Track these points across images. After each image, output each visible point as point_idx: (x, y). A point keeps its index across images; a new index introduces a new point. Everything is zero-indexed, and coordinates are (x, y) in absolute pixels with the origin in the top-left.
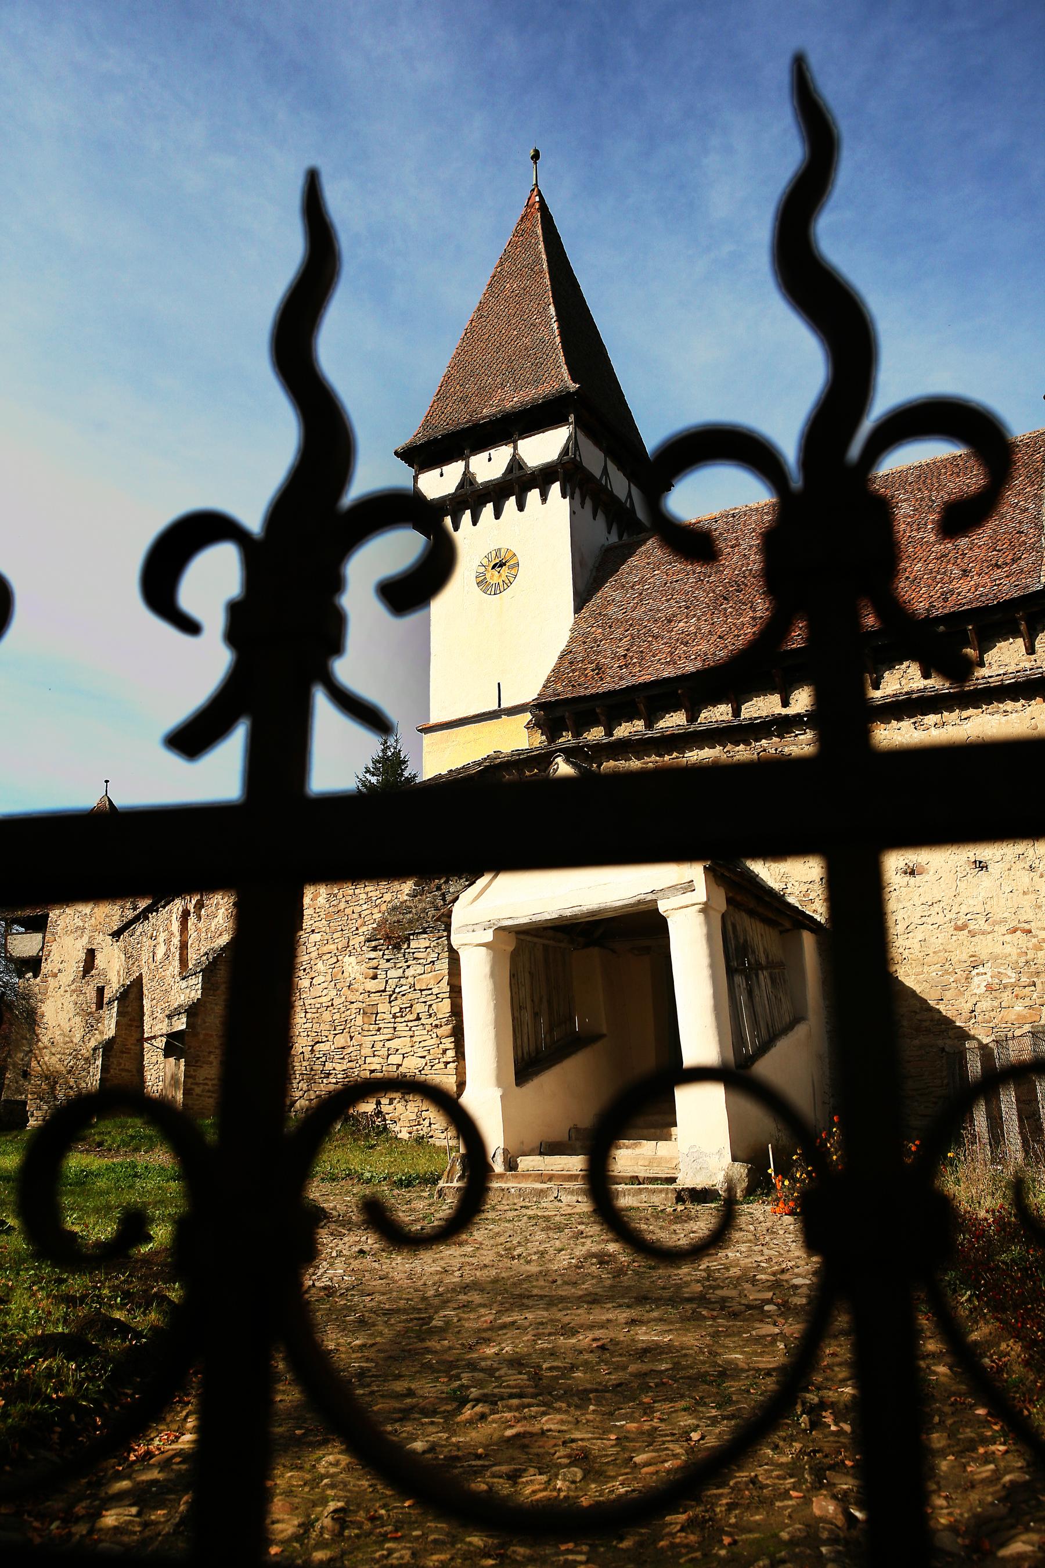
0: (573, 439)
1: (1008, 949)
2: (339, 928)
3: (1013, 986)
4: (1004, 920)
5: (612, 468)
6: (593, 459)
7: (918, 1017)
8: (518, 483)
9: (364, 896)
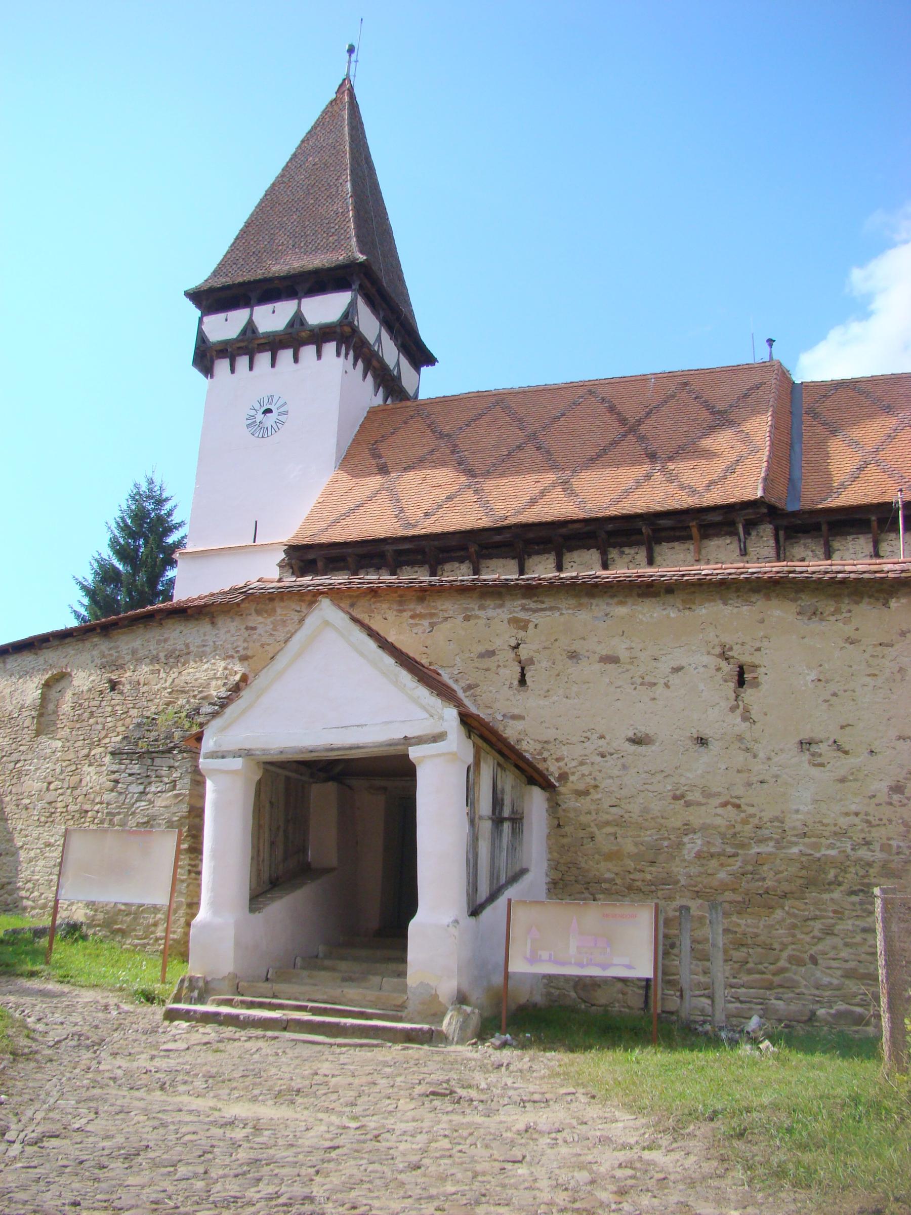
0: (352, 305)
1: (718, 821)
2: (82, 738)
3: (719, 854)
4: (719, 794)
5: (385, 336)
6: (369, 324)
7: (631, 876)
8: (297, 337)
9: (109, 709)
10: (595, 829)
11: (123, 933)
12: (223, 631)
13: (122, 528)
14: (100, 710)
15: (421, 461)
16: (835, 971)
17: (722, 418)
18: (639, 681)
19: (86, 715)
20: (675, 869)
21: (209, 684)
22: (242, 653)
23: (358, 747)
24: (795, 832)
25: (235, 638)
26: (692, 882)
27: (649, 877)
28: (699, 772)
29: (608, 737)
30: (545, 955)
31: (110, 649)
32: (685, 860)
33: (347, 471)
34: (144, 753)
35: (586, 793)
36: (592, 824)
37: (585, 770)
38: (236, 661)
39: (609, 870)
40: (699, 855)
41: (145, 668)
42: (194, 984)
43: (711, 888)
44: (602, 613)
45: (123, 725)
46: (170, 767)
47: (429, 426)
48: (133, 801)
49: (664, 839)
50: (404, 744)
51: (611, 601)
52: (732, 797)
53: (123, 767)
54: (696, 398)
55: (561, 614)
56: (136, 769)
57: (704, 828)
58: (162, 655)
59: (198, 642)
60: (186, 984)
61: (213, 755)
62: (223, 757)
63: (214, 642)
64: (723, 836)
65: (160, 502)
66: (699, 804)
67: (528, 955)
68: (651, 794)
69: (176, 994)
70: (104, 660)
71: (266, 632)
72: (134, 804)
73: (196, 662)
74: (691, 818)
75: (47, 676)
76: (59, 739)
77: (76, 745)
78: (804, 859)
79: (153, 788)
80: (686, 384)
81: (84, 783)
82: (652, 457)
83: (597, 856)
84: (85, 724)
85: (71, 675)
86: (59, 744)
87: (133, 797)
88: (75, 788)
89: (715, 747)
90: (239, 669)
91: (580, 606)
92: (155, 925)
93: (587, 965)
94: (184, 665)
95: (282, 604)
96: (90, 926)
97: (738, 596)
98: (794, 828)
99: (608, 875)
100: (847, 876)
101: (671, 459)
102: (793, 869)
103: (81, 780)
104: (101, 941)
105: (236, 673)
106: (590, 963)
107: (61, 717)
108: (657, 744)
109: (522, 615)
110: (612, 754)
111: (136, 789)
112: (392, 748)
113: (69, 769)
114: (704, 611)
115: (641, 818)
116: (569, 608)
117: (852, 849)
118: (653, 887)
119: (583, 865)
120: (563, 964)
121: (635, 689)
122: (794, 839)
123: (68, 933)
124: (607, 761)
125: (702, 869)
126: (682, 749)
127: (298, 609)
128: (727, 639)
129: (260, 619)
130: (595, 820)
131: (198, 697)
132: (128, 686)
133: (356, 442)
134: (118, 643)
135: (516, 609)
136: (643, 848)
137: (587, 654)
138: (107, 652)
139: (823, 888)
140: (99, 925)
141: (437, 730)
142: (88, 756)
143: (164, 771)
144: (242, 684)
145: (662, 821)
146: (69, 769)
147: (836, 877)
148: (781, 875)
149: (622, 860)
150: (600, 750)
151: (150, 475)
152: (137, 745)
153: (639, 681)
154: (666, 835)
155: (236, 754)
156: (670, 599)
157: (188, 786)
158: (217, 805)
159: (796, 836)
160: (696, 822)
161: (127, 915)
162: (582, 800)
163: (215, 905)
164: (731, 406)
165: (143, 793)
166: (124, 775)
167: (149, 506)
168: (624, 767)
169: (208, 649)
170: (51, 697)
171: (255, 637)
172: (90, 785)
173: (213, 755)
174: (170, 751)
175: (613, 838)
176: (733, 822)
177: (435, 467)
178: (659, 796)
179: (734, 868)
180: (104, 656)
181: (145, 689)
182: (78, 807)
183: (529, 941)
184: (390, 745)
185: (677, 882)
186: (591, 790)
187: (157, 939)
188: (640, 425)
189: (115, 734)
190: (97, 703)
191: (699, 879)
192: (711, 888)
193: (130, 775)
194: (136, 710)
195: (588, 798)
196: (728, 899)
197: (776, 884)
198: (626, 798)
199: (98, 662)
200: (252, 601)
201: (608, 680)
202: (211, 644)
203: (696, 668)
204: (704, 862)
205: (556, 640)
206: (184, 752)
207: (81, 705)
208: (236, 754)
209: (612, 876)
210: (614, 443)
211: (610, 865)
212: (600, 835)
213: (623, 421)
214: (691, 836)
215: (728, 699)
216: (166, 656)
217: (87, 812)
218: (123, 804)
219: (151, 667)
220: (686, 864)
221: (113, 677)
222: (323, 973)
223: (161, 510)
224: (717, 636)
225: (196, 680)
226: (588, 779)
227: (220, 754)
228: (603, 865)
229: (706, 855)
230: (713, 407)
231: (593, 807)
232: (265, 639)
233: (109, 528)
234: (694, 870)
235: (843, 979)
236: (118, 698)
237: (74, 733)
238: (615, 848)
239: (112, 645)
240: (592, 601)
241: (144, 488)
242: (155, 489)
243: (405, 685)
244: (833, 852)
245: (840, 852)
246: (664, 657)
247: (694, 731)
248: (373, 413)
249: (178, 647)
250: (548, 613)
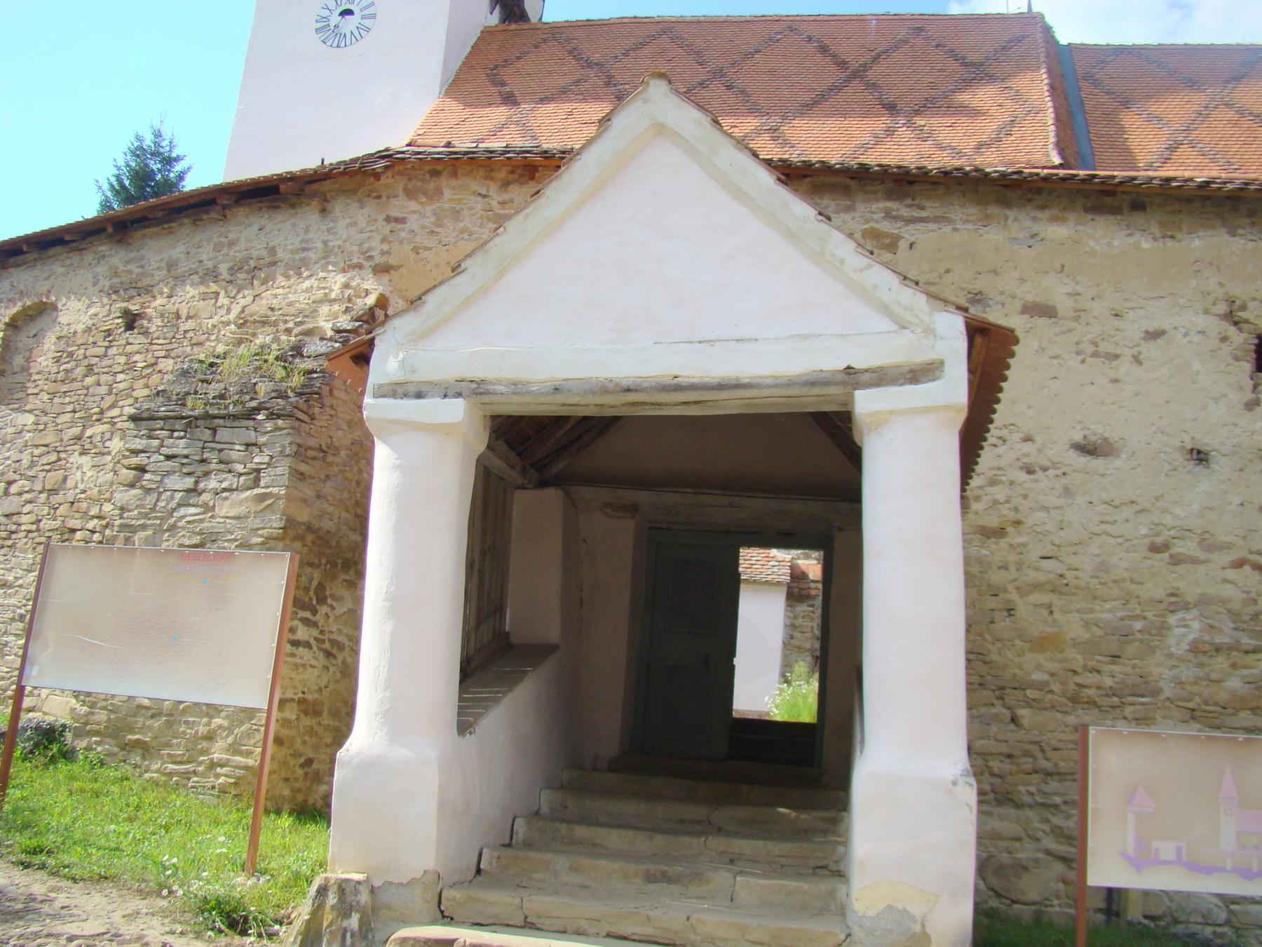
1: (1228, 591)
2: (70, 408)
4: (1227, 546)
7: (1079, 680)
9: (122, 360)
10: (1014, 596)
11: (145, 749)
12: (341, 225)
13: (117, 192)
14: (106, 362)
15: (564, 93)
17: (978, 72)
18: (1090, 349)
19: (80, 371)
20: (1156, 671)
21: (315, 311)
22: (378, 259)
23: (738, 386)
25: (367, 235)
26: (1184, 693)
27: (1108, 682)
28: (1195, 507)
29: (1039, 440)
30: (1167, 850)
31: (128, 262)
32: (1170, 656)
33: (456, 99)
34: (196, 418)
35: (1000, 532)
36: (1010, 587)
37: (999, 493)
38: (368, 273)
39: (1038, 667)
40: (1195, 648)
41: (191, 291)
42: (350, 898)
43: (1216, 704)
44: (1021, 235)
45: (147, 386)
46: (248, 445)
47: (570, 52)
48: (173, 504)
49: (1136, 617)
50: (843, 383)
51: (1039, 214)
52: (1251, 552)
53: (156, 443)
54: (937, 46)
55: (955, 230)
56: (180, 446)
57: (1204, 602)
58: (223, 268)
59: (294, 242)
60: (332, 899)
61: (396, 390)
62: (419, 396)
63: (325, 243)
64: (1234, 615)
65: (169, 161)
66: (1196, 561)
67: (1130, 850)
68: (1112, 541)
69: (308, 922)
70: (115, 280)
71: (423, 227)
72: (174, 510)
73: (288, 277)
74: (1181, 585)
75: (14, 311)
76: (30, 412)
77: (58, 421)
79: (212, 483)
80: (920, 29)
81: (70, 483)
82: (891, 108)
83: (1018, 642)
84: (76, 385)
85: (55, 308)
86: (30, 419)
87: (172, 498)
88: (53, 491)
89: (1222, 466)
90: (371, 289)
91: (986, 219)
92: (210, 737)
94: (265, 282)
95: (454, 182)
96: (79, 734)
97: (1253, 224)
99: (1037, 676)
101: (917, 113)
103: (65, 479)
104: (102, 764)
105: (367, 293)
107: (35, 377)
108: (1124, 456)
109: (886, 227)
110: (1045, 469)
111: (179, 483)
112: (816, 391)
113: (45, 460)
114: (1197, 243)
115: (1095, 581)
116: (967, 221)
118: (1115, 699)
119: (994, 657)
121: (1083, 362)
123: (36, 745)
124: (1036, 481)
125: (1201, 673)
126: (1167, 467)
127: (484, 192)
128: (1238, 290)
129: (413, 205)
130: (1015, 580)
131: (297, 330)
132: (158, 322)
133: (469, 65)
134: (143, 252)
135: (875, 217)
136: (1099, 632)
137: (1002, 298)
138: (121, 267)
140: (97, 733)
141: (921, 357)
142: (79, 438)
143: (237, 452)
144: (379, 313)
145: (1132, 587)
146: (45, 460)
149: (1062, 651)
150: (1026, 460)
151: (157, 125)
152: (184, 405)
153: (1090, 349)
154: (1138, 612)
155: (449, 391)
156: (1139, 219)
157: (285, 480)
158: (402, 498)
160: (1191, 592)
161: (153, 717)
162: (992, 544)
163: (391, 718)
164: (987, 59)
165: (194, 491)
166: (155, 457)
167: (155, 166)
168: (1067, 492)
169: (311, 254)
170: (20, 345)
171: (403, 234)
172: (81, 486)
173: (396, 390)
174: (250, 415)
175: (1045, 613)
176: (1253, 595)
177: (585, 100)
178: (1126, 545)
180: (116, 274)
181: (190, 324)
182: (58, 523)
183: (1131, 818)
184: (813, 384)
185: (1157, 692)
186: (1010, 529)
187: (213, 765)
188: (865, 71)
189: (131, 401)
190: (100, 351)
191: (1195, 689)
192: (1216, 704)
193: (169, 457)
194: (171, 361)
195: (1003, 542)
196: (1246, 724)
198: (1070, 545)
199: (105, 283)
200: (400, 174)
201: (1036, 345)
202: (320, 245)
203: (1186, 335)
205: (947, 271)
206: (279, 416)
207: (71, 354)
208: (449, 391)
209: (1046, 677)
210: (834, 89)
211: (1041, 658)
212: (1024, 607)
213: (842, 64)
214: (1181, 615)
215: (1241, 389)
216: (231, 269)
217: (73, 531)
218: (153, 509)
219: (203, 289)
220: (1174, 662)
221: (132, 308)
222: (603, 863)
223: (169, 171)
224: (1221, 285)
225: (290, 304)
226: (1004, 510)
227: (412, 389)
228: (1030, 659)
229: (1207, 647)
230: (963, 58)
231: (1012, 558)
232: (422, 239)
233: (100, 188)
234: (1187, 673)
236: (137, 339)
237: (56, 400)
238: (1050, 630)
239: (132, 255)
240: (1008, 212)
241: (148, 141)
242: (164, 144)
243: (842, 262)
246: (1131, 313)
247: (1187, 438)
248: (487, 33)
249: (255, 254)
250: (931, 226)
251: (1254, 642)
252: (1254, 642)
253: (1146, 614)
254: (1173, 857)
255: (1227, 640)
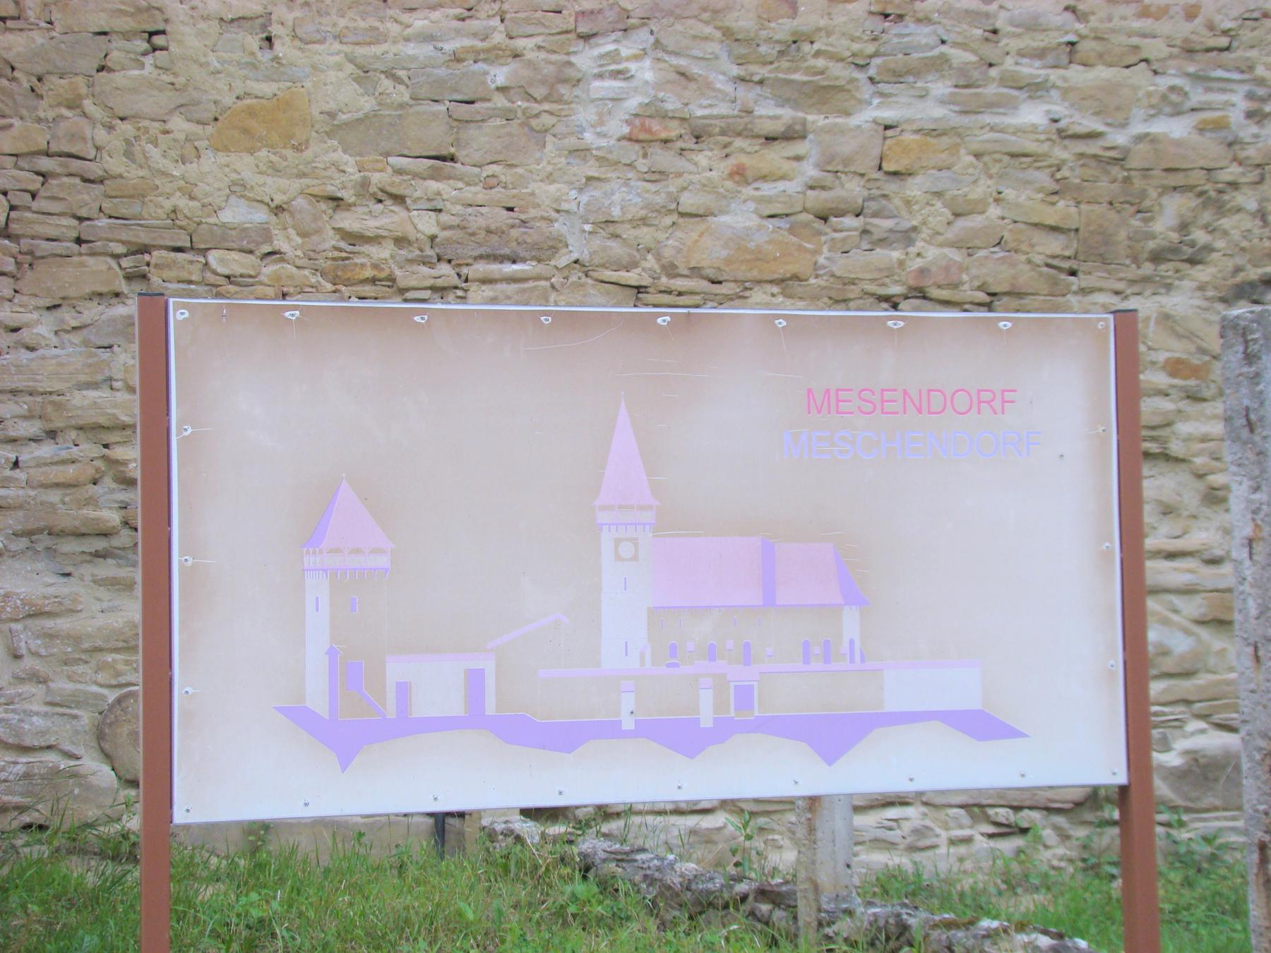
7: (348, 221)
16: (1176, 600)
20: (546, 192)
24: (1038, 41)
26: (616, 249)
27: (427, 224)
30: (436, 686)
32: (581, 152)
39: (238, 189)
49: (493, 55)
67: (317, 699)
78: (1060, 153)
83: (179, 125)
93: (723, 731)
98: (1032, 26)
99: (236, 214)
100: (1225, 223)
102: (1025, 197)
106: (743, 719)
117: (1250, 115)
118: (444, 269)
119: (115, 164)
120: (565, 737)
122: (1031, 70)
125: (658, 195)
136: (401, 94)
139: (1133, 272)
147: (1184, 227)
148: (975, 222)
154: (499, 38)
159: (1040, 54)
175: (253, 42)
179: (792, 187)
183: (317, 590)
191: (645, 235)
192: (696, 272)
197: (956, 256)
204: (663, 158)
211: (244, 166)
228: (211, 169)
229: (674, 129)
234: (623, 197)
235: (1204, 633)
238: (267, 88)
244: (1176, 129)
245: (1201, 129)
251: (787, 114)
252: (787, 114)
253: (520, 43)
254: (455, 706)
255: (723, 109)
